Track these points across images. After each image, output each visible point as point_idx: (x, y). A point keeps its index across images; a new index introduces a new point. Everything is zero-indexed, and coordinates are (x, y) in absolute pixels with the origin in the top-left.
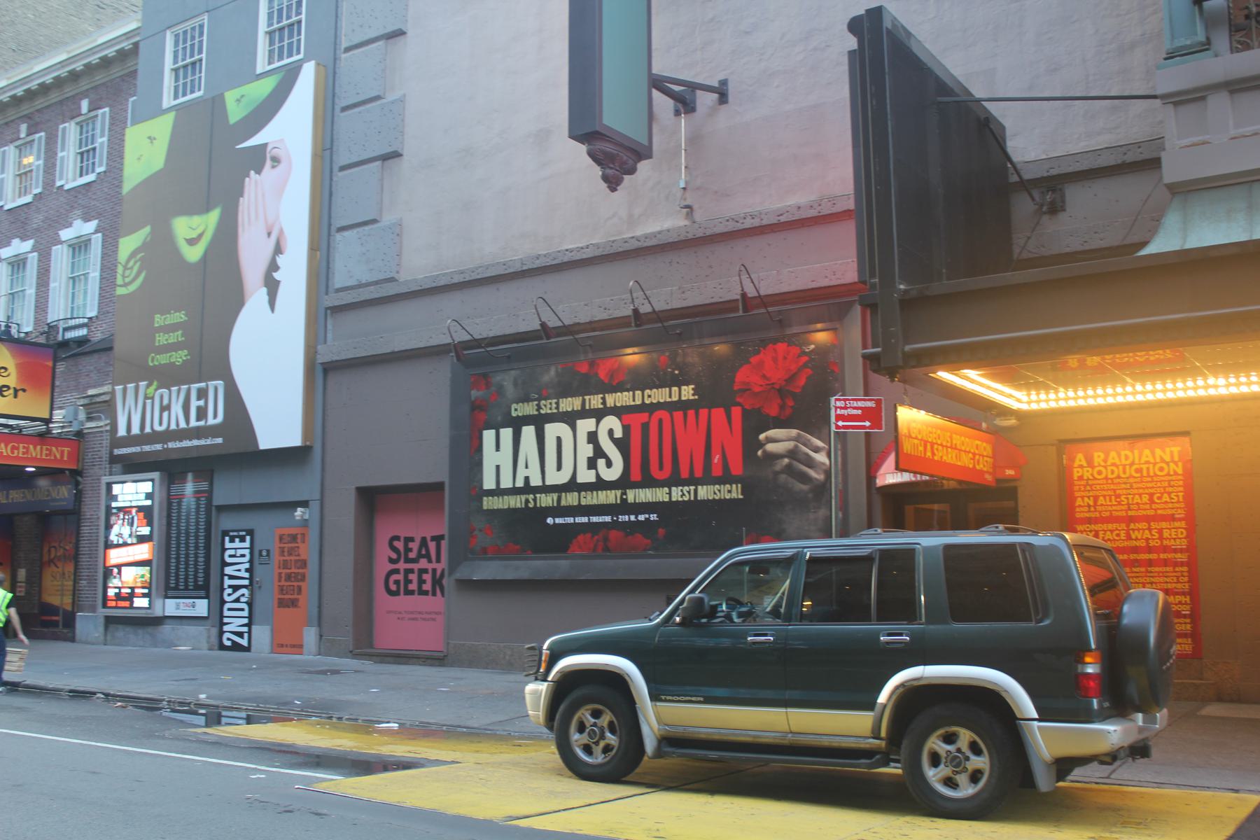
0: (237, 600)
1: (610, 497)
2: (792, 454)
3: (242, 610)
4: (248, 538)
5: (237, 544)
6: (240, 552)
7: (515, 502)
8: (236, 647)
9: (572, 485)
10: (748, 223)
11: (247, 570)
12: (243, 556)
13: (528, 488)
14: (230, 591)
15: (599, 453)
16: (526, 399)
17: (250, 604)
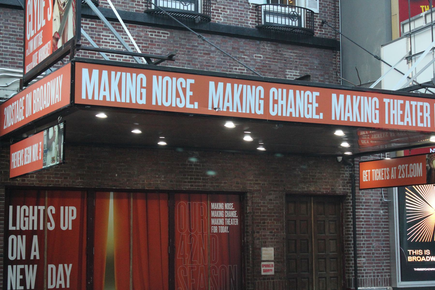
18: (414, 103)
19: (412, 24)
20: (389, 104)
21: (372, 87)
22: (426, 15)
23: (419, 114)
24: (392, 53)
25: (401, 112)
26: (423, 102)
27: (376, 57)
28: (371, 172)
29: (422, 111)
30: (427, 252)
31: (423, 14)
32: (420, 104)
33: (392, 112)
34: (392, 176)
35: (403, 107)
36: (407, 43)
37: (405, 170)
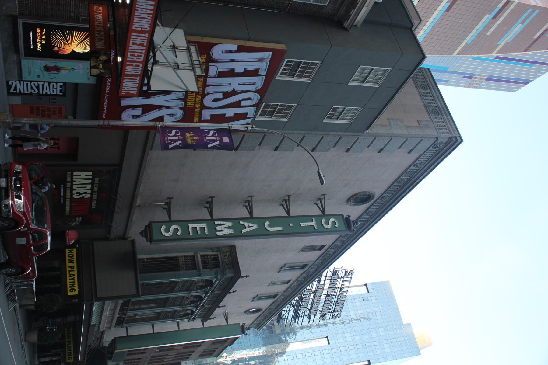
0: (32, 88)
1: (68, 195)
2: (75, 221)
3: (28, 91)
4: (62, 94)
5: (59, 89)
6: (55, 90)
7: (69, 179)
8: (9, 87)
9: (72, 189)
10: (131, 215)
11: (46, 93)
12: (53, 91)
13: (72, 181)
14: (36, 85)
15: (80, 194)
16: (100, 181)
17: (31, 93)
18: (144, 52)
19: (195, 51)
20: (145, 37)
21: (158, 22)
22: (199, 61)
23: (136, 54)
24: (179, 37)
25: (138, 43)
26: (144, 57)
27: (177, 25)
28: (100, 13)
29: (138, 56)
30: (44, 42)
31: (200, 59)
32: (143, 55)
33: (139, 38)
34: (97, 27)
35: (142, 45)
36: (183, 47)
37: (100, 36)
